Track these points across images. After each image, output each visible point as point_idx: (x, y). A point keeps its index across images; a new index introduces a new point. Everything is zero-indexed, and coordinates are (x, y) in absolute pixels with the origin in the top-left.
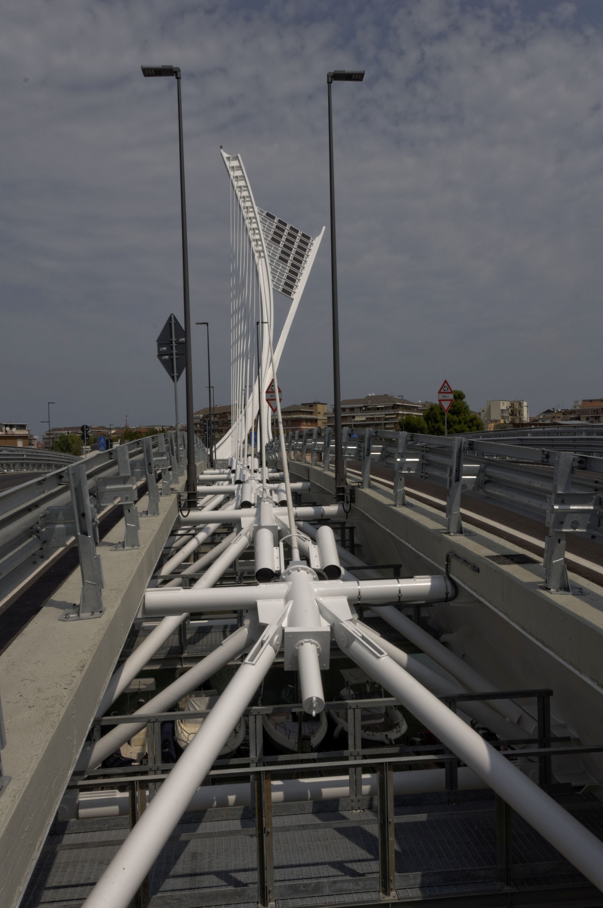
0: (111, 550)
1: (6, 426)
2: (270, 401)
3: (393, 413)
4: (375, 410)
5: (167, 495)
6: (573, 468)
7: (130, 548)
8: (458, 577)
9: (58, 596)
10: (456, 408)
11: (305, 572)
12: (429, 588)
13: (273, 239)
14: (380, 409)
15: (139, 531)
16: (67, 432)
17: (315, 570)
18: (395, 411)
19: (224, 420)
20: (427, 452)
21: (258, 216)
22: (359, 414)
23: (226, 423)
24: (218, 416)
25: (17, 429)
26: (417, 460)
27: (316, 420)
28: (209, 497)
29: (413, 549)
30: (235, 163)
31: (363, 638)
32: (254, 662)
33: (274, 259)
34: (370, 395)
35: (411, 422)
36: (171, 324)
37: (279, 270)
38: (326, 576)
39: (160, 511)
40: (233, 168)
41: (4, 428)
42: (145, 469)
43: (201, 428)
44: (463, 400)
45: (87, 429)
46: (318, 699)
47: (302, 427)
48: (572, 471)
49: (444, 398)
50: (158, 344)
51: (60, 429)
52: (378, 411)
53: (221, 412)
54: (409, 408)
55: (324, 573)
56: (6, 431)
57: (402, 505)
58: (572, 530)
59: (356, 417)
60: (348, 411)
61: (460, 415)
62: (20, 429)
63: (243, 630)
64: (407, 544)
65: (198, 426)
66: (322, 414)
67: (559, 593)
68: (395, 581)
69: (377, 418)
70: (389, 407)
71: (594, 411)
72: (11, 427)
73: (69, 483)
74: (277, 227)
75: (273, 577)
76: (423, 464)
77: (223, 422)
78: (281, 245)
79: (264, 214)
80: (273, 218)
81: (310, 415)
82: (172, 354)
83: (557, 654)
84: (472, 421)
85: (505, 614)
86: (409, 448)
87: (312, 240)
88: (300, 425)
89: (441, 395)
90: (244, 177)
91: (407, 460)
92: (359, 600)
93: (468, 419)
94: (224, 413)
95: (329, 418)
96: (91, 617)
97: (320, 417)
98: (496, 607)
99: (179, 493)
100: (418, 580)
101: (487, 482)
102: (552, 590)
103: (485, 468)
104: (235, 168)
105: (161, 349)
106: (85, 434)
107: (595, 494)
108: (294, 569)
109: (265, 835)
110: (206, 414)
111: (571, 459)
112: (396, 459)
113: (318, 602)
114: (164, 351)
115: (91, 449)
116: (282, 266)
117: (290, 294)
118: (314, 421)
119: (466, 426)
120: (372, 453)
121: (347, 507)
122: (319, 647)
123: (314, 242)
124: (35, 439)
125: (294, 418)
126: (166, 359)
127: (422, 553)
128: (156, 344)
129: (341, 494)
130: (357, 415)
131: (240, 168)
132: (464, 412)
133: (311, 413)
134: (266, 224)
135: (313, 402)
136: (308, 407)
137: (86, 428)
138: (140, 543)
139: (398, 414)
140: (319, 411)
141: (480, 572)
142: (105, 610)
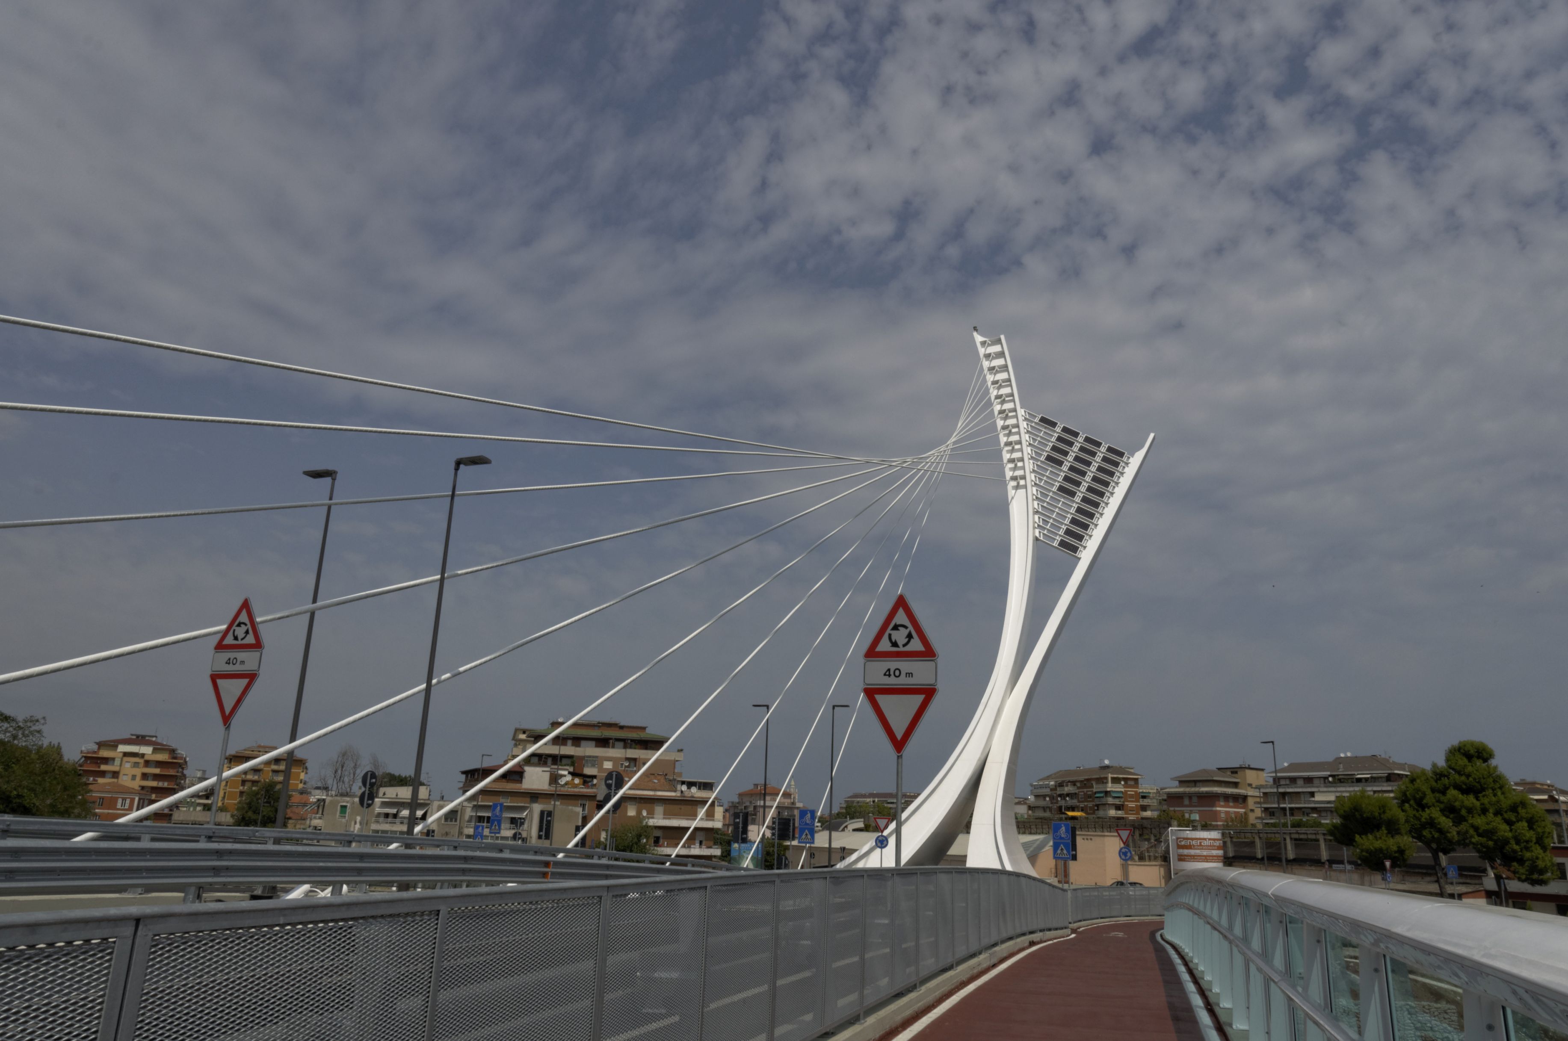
1: (683, 783)
3: (1389, 788)
4: (1353, 782)
10: (1471, 779)
13: (1049, 458)
14: (1363, 780)
16: (872, 800)
19: (1087, 791)
21: (1023, 425)
22: (1321, 789)
23: (1090, 797)
24: (1078, 784)
27: (1245, 798)
33: (1050, 491)
34: (1342, 755)
35: (1364, 806)
43: (1052, 803)
44: (1489, 762)
45: (374, 780)
47: (1218, 809)
49: (892, 681)
51: (864, 796)
52: (1359, 784)
53: (1082, 778)
56: (682, 792)
59: (1316, 794)
61: (1483, 796)
62: (704, 789)
65: (1048, 799)
70: (1381, 778)
72: (690, 784)
77: (1085, 794)
80: (1054, 424)
81: (1233, 788)
84: (1514, 808)
87: (1129, 458)
88: (1213, 805)
93: (1505, 803)
94: (1088, 780)
95: (1265, 794)
97: (1250, 792)
110: (1060, 780)
115: (820, 828)
116: (1063, 502)
117: (1075, 549)
118: (1242, 799)
119: (1498, 819)
123: (1131, 460)
125: (1202, 793)
130: (1319, 792)
131: (1001, 355)
133: (1236, 785)
135: (1238, 766)
136: (1229, 773)
137: (371, 778)
140: (1249, 781)
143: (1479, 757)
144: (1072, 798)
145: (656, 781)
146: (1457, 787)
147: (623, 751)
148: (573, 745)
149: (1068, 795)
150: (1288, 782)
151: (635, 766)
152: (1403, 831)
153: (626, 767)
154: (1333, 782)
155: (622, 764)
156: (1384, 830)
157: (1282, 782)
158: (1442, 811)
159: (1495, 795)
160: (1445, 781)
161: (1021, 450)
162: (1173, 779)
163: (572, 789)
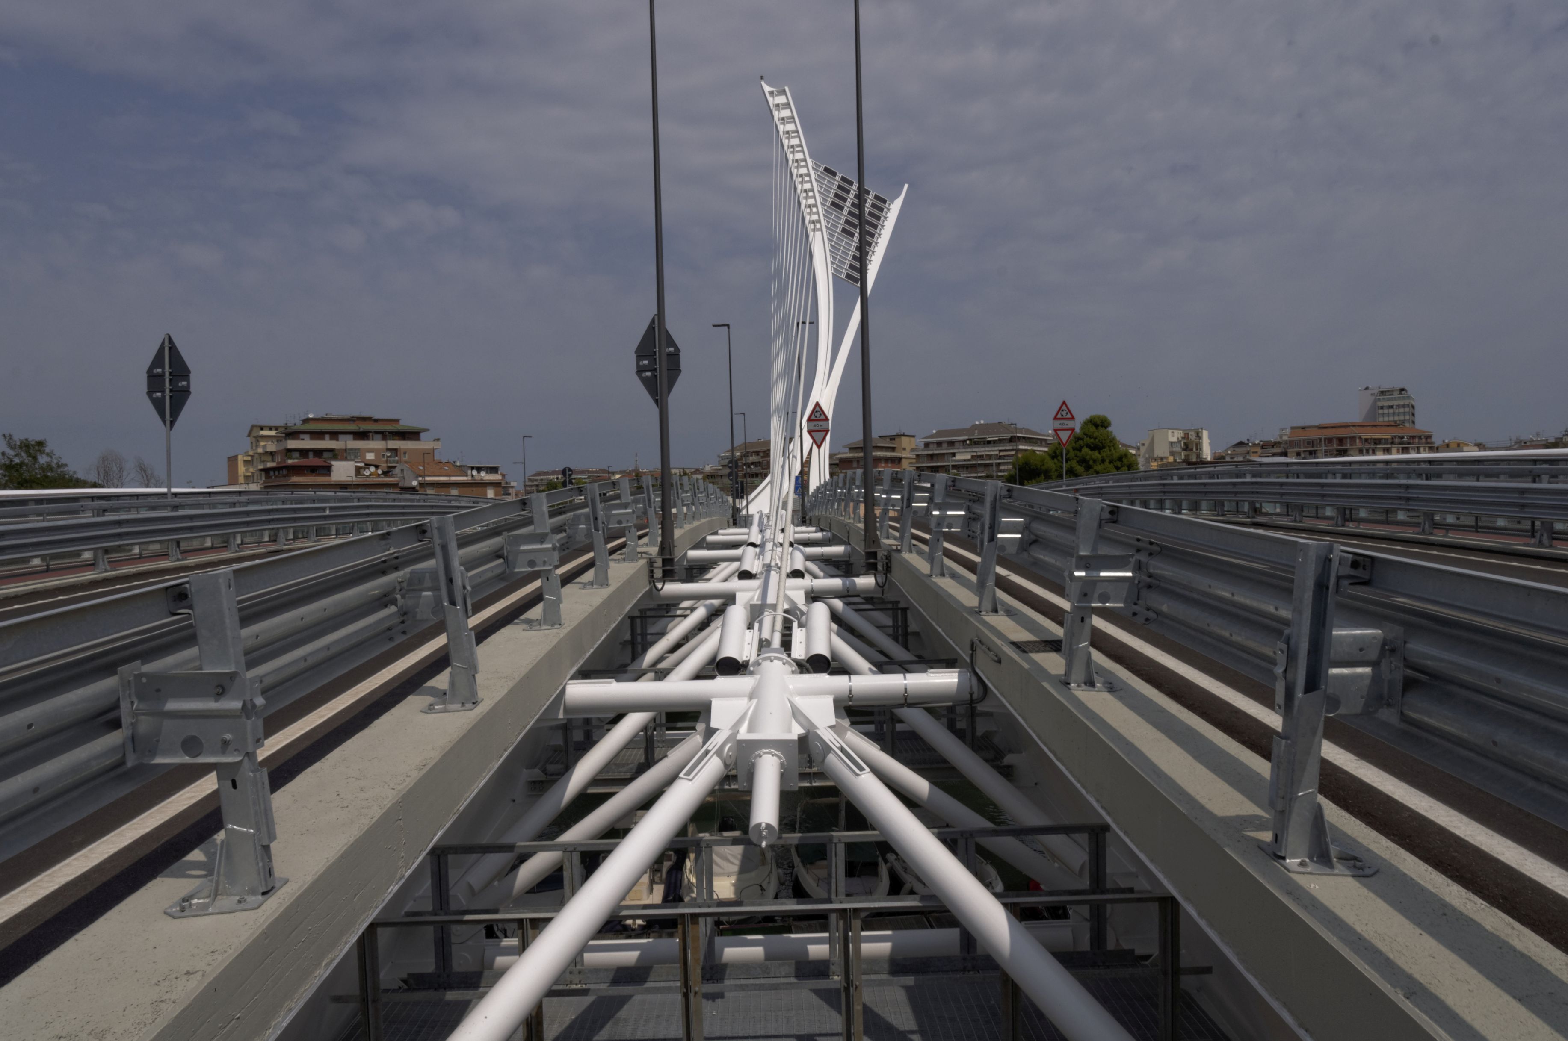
0: (524, 630)
1: (472, 468)
2: (812, 433)
3: (1011, 448)
5: (632, 560)
6: (1101, 520)
7: (549, 627)
8: (982, 672)
9: (431, 683)
11: (780, 663)
12: (956, 686)
13: (833, 204)
15: (561, 605)
16: (555, 476)
17: (795, 660)
18: (1013, 446)
20: (974, 502)
21: (812, 173)
22: (961, 450)
24: (761, 454)
25: (487, 473)
26: (963, 513)
27: (900, 460)
28: (723, 565)
29: (943, 634)
30: (781, 100)
31: (842, 749)
32: (690, 777)
33: (835, 232)
34: (977, 423)
36: (654, 328)
37: (842, 248)
38: (811, 669)
39: (610, 582)
40: (778, 106)
41: (469, 472)
42: (590, 525)
46: (768, 826)
48: (1100, 526)
50: (637, 356)
54: (1034, 441)
55: (808, 665)
56: (472, 476)
57: (941, 575)
58: (1100, 605)
60: (945, 445)
63: (695, 738)
64: (938, 628)
66: (908, 449)
67: (1080, 688)
68: (901, 676)
69: (987, 455)
70: (1005, 439)
71: (1308, 443)
72: (479, 469)
73: (432, 538)
74: (840, 187)
75: (739, 669)
76: (970, 518)
78: (845, 212)
79: (821, 169)
82: (655, 370)
83: (1067, 769)
84: (1120, 459)
85: (1024, 719)
86: (948, 494)
87: (890, 204)
89: (1058, 422)
90: (793, 118)
91: (949, 513)
92: (851, 701)
93: (1116, 455)
95: (918, 456)
96: (460, 709)
97: (904, 455)
98: (1015, 710)
99: (650, 559)
100: (932, 675)
101: (1035, 542)
102: (1072, 685)
103: (1030, 523)
104: (780, 106)
105: (641, 363)
106: (567, 480)
107: (1132, 556)
108: (765, 659)
109: (691, 995)
111: (1098, 508)
112: (931, 513)
113: (790, 702)
114: (644, 365)
120: (913, 505)
121: (880, 580)
122: (783, 759)
123: (892, 206)
124: (512, 487)
126: (647, 377)
127: (951, 639)
128: (634, 356)
129: (872, 561)
130: (959, 452)
131: (787, 106)
132: (1109, 447)
133: (893, 449)
134: (823, 184)
135: (895, 434)
136: (888, 440)
138: (563, 622)
139: (1018, 451)
140: (903, 446)
141: (1002, 662)
142: (481, 701)
143: (1102, 426)
144: (756, 466)
145: (446, 468)
146: (1088, 446)
147: (383, 442)
148: (331, 439)
149: (752, 463)
150: (935, 445)
151: (397, 456)
152: (1054, 477)
153: (388, 457)
154: (970, 444)
155: (384, 455)
156: (1043, 477)
157: (931, 446)
158: (1078, 462)
159: (1110, 451)
160: (1081, 442)
161: (814, 197)
162: (844, 447)
163: (377, 479)
